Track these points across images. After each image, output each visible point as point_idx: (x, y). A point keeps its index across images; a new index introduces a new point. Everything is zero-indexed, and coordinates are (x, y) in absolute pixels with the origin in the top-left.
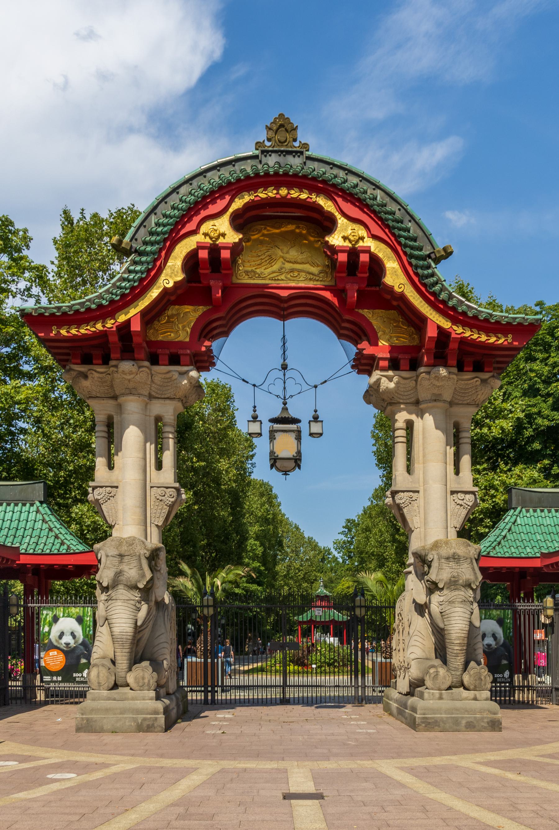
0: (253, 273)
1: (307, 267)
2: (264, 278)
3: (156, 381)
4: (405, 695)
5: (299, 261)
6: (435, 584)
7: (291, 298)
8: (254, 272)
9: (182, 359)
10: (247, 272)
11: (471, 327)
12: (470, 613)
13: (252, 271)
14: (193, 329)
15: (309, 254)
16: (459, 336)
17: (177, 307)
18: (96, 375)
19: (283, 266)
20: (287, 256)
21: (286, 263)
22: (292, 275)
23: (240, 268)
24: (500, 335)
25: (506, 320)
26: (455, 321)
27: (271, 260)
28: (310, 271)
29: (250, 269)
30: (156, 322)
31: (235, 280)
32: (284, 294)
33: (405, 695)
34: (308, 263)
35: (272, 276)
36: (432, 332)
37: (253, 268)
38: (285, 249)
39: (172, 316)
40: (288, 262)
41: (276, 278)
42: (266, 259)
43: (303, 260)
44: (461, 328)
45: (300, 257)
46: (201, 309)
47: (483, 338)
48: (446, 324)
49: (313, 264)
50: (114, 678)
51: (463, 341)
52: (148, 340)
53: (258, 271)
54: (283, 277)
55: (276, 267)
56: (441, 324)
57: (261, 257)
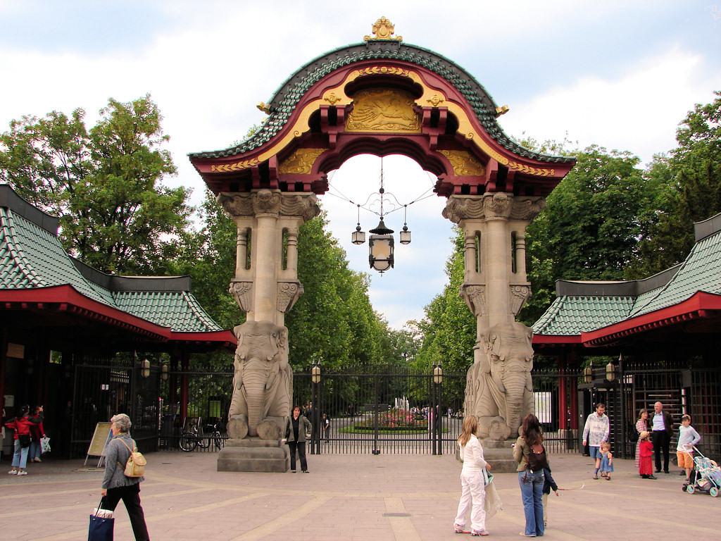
2: (367, 129)
5: (394, 115)
6: (498, 357)
7: (389, 141)
9: (307, 187)
11: (523, 163)
15: (402, 112)
16: (514, 170)
17: (302, 149)
18: (240, 199)
24: (545, 170)
26: (511, 159)
27: (374, 115)
29: (358, 122)
30: (287, 161)
36: (493, 167)
38: (384, 108)
39: (299, 155)
44: (515, 164)
45: (395, 114)
46: (321, 151)
47: (533, 171)
48: (504, 161)
49: (405, 119)
50: (247, 430)
51: (518, 174)
54: (382, 127)
55: (377, 121)
56: (501, 162)
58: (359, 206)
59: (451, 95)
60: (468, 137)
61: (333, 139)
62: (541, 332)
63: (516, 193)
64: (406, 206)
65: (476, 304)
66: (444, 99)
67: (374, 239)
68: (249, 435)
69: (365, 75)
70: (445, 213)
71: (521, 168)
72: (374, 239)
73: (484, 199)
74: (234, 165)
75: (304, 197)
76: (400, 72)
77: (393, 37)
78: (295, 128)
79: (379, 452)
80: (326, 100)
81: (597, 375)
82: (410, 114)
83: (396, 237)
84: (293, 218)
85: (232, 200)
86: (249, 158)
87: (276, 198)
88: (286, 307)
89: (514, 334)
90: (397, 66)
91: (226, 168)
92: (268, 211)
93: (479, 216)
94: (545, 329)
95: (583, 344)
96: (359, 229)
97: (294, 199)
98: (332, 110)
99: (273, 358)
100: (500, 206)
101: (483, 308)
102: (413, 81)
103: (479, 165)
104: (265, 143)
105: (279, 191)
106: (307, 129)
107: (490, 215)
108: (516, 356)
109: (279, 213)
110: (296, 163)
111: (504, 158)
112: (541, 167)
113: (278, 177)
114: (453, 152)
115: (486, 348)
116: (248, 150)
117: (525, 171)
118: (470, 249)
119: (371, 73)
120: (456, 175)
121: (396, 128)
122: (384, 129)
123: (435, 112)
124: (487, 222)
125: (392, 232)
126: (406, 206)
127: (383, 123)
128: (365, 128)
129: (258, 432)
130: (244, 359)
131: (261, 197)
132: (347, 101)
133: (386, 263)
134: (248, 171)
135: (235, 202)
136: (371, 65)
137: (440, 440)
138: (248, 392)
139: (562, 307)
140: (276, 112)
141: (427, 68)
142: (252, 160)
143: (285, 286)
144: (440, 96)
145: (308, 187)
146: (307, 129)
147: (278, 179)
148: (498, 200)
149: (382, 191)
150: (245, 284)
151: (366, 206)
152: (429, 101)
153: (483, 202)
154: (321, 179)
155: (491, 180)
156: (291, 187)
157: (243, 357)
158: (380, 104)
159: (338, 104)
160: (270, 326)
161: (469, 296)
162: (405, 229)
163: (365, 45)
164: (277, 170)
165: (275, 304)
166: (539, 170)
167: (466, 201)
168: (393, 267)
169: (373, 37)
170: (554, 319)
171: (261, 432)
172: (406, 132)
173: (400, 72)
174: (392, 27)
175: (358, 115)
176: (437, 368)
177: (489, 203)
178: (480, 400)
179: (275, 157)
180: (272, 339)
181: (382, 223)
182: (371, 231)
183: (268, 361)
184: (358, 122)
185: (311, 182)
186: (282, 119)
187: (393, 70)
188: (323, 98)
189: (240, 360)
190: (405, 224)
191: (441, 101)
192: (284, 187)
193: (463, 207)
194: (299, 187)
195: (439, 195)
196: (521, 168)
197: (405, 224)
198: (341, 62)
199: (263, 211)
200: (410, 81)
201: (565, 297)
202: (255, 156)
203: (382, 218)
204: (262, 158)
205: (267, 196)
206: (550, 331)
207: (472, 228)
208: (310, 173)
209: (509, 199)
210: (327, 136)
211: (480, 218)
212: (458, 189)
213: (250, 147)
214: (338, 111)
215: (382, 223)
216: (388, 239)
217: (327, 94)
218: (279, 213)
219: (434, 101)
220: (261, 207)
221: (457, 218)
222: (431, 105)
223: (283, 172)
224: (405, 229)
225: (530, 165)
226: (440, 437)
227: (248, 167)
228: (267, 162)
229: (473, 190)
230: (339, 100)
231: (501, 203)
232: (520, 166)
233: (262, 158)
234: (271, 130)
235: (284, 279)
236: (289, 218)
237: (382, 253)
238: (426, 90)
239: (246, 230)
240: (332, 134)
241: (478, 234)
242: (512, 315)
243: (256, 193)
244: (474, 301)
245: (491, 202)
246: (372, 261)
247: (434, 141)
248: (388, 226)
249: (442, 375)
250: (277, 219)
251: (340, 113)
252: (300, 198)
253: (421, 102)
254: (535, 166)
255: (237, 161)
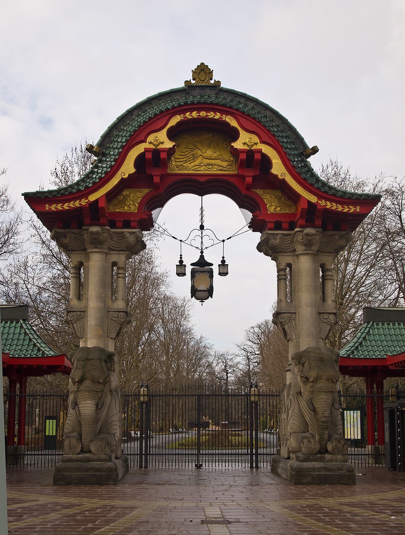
0: (181, 167)
1: (218, 162)
3: (114, 239)
4: (287, 459)
5: (213, 158)
8: (182, 166)
9: (132, 224)
10: (177, 167)
11: (331, 201)
12: (332, 399)
13: (181, 165)
14: (139, 204)
15: (220, 153)
17: (129, 190)
19: (202, 161)
20: (205, 155)
21: (204, 159)
22: (208, 167)
23: (173, 163)
24: (351, 207)
25: (356, 196)
26: (320, 197)
27: (194, 158)
28: (221, 165)
29: (179, 163)
31: (169, 171)
32: (203, 180)
33: (287, 459)
34: (219, 159)
35: (194, 168)
37: (182, 163)
38: (204, 150)
39: (126, 194)
40: (205, 158)
41: (197, 169)
42: (191, 157)
43: (216, 158)
44: (324, 201)
46: (146, 191)
47: (340, 208)
48: (313, 199)
50: (81, 446)
51: (326, 211)
52: (109, 212)
53: (185, 165)
55: (197, 162)
56: (311, 200)
57: (187, 156)
58: (181, 241)
59: (266, 139)
60: (280, 177)
61: (157, 180)
62: (349, 355)
63: (324, 228)
64: (223, 241)
65: (288, 331)
66: (259, 141)
67: (196, 272)
68: (82, 451)
69: (186, 119)
70: (260, 248)
71: (329, 205)
72: (196, 272)
73: (295, 234)
74: (67, 204)
75: (131, 233)
76: (218, 116)
77: (212, 82)
78: (122, 169)
79: (201, 465)
80: (150, 143)
81: (401, 395)
82: (227, 156)
83: (216, 269)
84: (121, 252)
85: (65, 237)
86: (80, 198)
87: (105, 235)
88: (115, 334)
89: (322, 358)
90: (215, 111)
91: (59, 207)
92: (99, 246)
93: (288, 251)
94: (353, 352)
95: (388, 366)
96: (181, 262)
97: (122, 235)
98: (156, 152)
99: (104, 381)
100: (309, 241)
101: (293, 334)
102: (230, 124)
103: (289, 203)
104: (94, 183)
105: (108, 228)
106: (133, 170)
107: (300, 249)
108: (324, 377)
109: (109, 248)
110: (123, 203)
111: (313, 196)
112: (348, 204)
113: (107, 215)
114: (266, 190)
115: (296, 370)
116: (79, 191)
117: (332, 208)
118: (283, 281)
119: (191, 117)
120: (269, 212)
121: (215, 170)
122: (203, 170)
123: (250, 153)
124: (298, 256)
125: (212, 265)
126: (223, 241)
127: (202, 164)
128: (186, 169)
129: (91, 448)
130: (78, 382)
131: (92, 233)
132: (169, 144)
133: (206, 294)
134: (81, 209)
135: (68, 238)
136: (191, 111)
137: (257, 454)
138: (81, 411)
139: (369, 331)
140: (104, 155)
141: (243, 113)
142: (83, 200)
143: (115, 314)
144: (255, 139)
145: (135, 224)
146: (133, 170)
147: (107, 217)
148: (307, 235)
149: (202, 227)
150: (78, 313)
151: (187, 242)
152: (244, 144)
153: (294, 237)
154: (147, 217)
155: (301, 217)
156: (121, 224)
157: (77, 380)
158: (199, 146)
159: (161, 146)
160: (101, 350)
161: (281, 323)
162: (223, 261)
163: (185, 90)
164: (106, 209)
165: (106, 331)
166: (346, 207)
167: (278, 237)
168: (212, 297)
169: (193, 82)
170: (361, 343)
171: (93, 449)
172: (224, 172)
173: (218, 116)
174: (211, 72)
175: (180, 157)
176: (253, 389)
177: (299, 237)
178: (292, 418)
179: (104, 196)
180: (103, 364)
181: (202, 257)
182: (192, 265)
183: (100, 383)
184: (179, 163)
185: (137, 219)
186: (110, 161)
187: (211, 115)
188: (147, 141)
189: (74, 382)
190: (223, 257)
191: (256, 144)
192: (113, 225)
193: (276, 241)
194: (127, 224)
195: (253, 231)
196: (329, 205)
197: (223, 257)
198: (163, 107)
199: (93, 246)
200: (228, 124)
201: (371, 323)
202: (86, 196)
203: (202, 252)
204: (93, 198)
205: (97, 233)
206: (357, 355)
207: (286, 259)
208: (136, 211)
209: (318, 233)
210: (151, 177)
211: (292, 251)
212: (272, 225)
213: (81, 188)
214: (161, 153)
215: (202, 257)
216: (208, 272)
217: (151, 138)
218: (109, 248)
219: (250, 144)
220: (92, 243)
221: (270, 252)
222: (246, 147)
223: (112, 210)
224: (223, 261)
225: (337, 202)
226: (257, 451)
227: (79, 206)
228: (97, 201)
229: (285, 225)
230: (162, 143)
231: (310, 238)
232: (329, 203)
233: (93, 198)
234: (100, 171)
235: (113, 309)
236: (117, 252)
237: (202, 287)
238: (243, 134)
239: (78, 264)
240: (155, 175)
241: (289, 265)
242: (321, 340)
243: (88, 229)
244: (286, 327)
245: (301, 237)
246: (194, 292)
247: (249, 180)
248: (208, 259)
249: (259, 395)
250: (107, 254)
251: (163, 155)
252: (127, 235)
253: (238, 145)
254: (342, 204)
255: (69, 201)
